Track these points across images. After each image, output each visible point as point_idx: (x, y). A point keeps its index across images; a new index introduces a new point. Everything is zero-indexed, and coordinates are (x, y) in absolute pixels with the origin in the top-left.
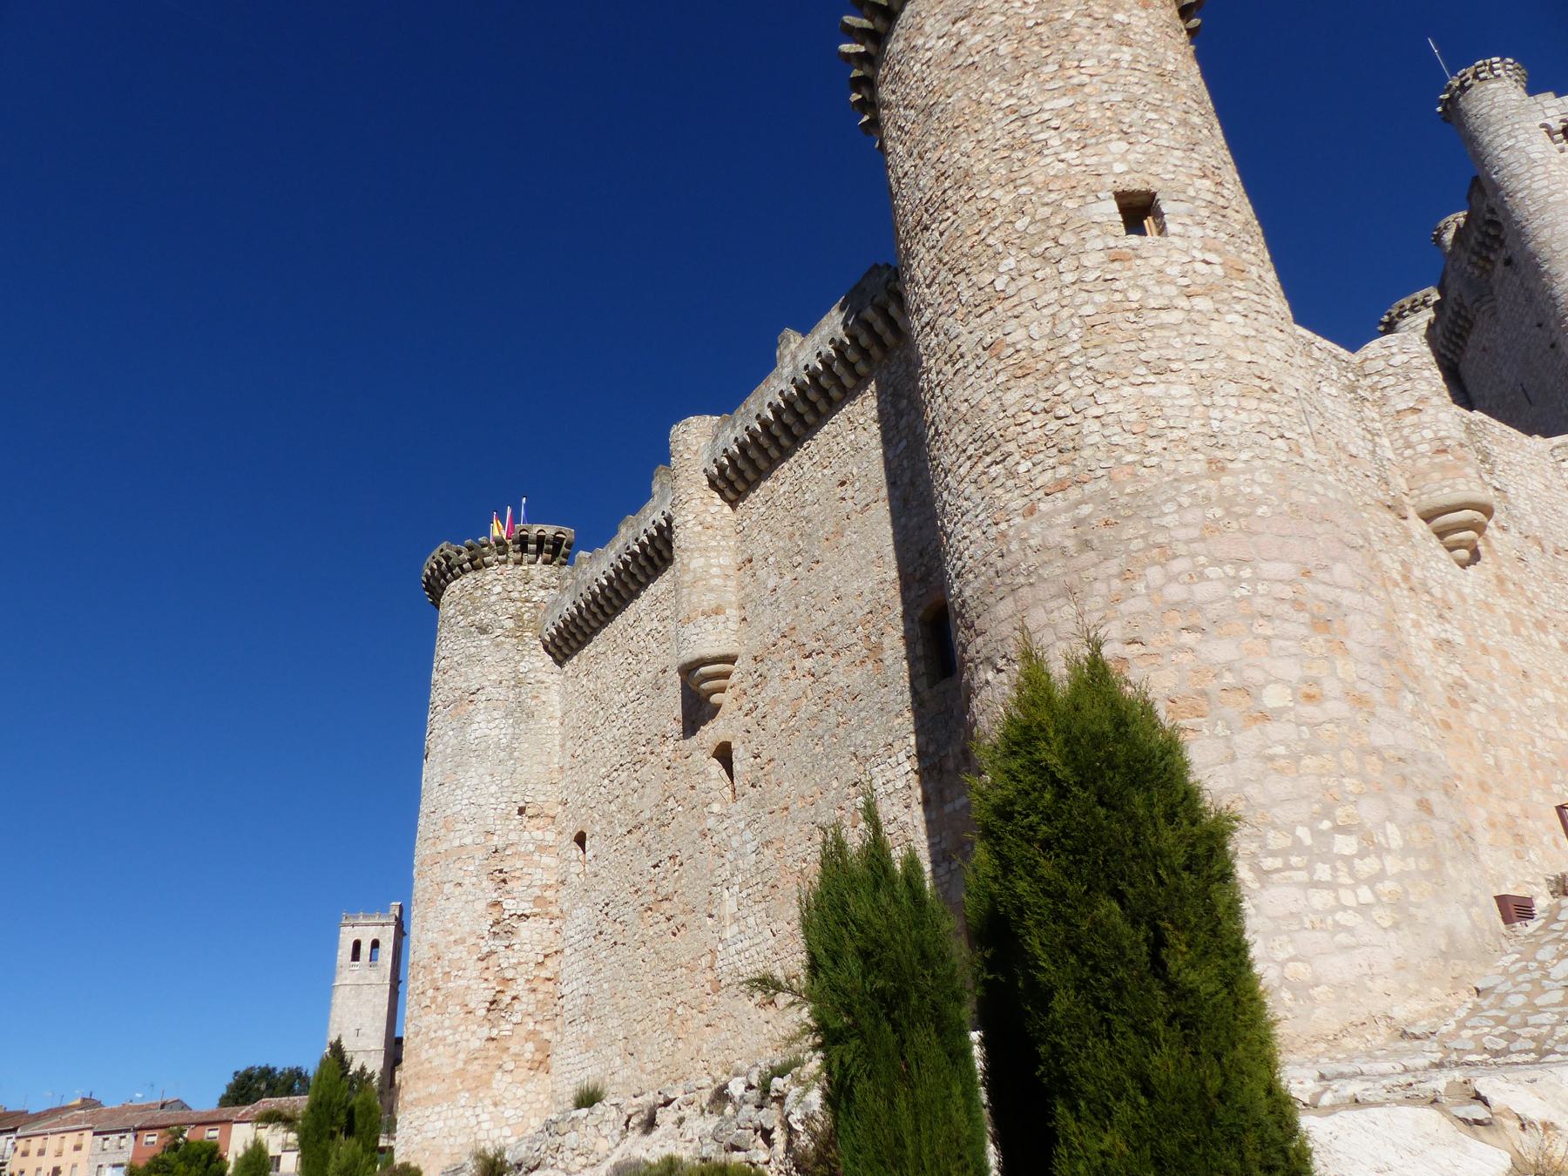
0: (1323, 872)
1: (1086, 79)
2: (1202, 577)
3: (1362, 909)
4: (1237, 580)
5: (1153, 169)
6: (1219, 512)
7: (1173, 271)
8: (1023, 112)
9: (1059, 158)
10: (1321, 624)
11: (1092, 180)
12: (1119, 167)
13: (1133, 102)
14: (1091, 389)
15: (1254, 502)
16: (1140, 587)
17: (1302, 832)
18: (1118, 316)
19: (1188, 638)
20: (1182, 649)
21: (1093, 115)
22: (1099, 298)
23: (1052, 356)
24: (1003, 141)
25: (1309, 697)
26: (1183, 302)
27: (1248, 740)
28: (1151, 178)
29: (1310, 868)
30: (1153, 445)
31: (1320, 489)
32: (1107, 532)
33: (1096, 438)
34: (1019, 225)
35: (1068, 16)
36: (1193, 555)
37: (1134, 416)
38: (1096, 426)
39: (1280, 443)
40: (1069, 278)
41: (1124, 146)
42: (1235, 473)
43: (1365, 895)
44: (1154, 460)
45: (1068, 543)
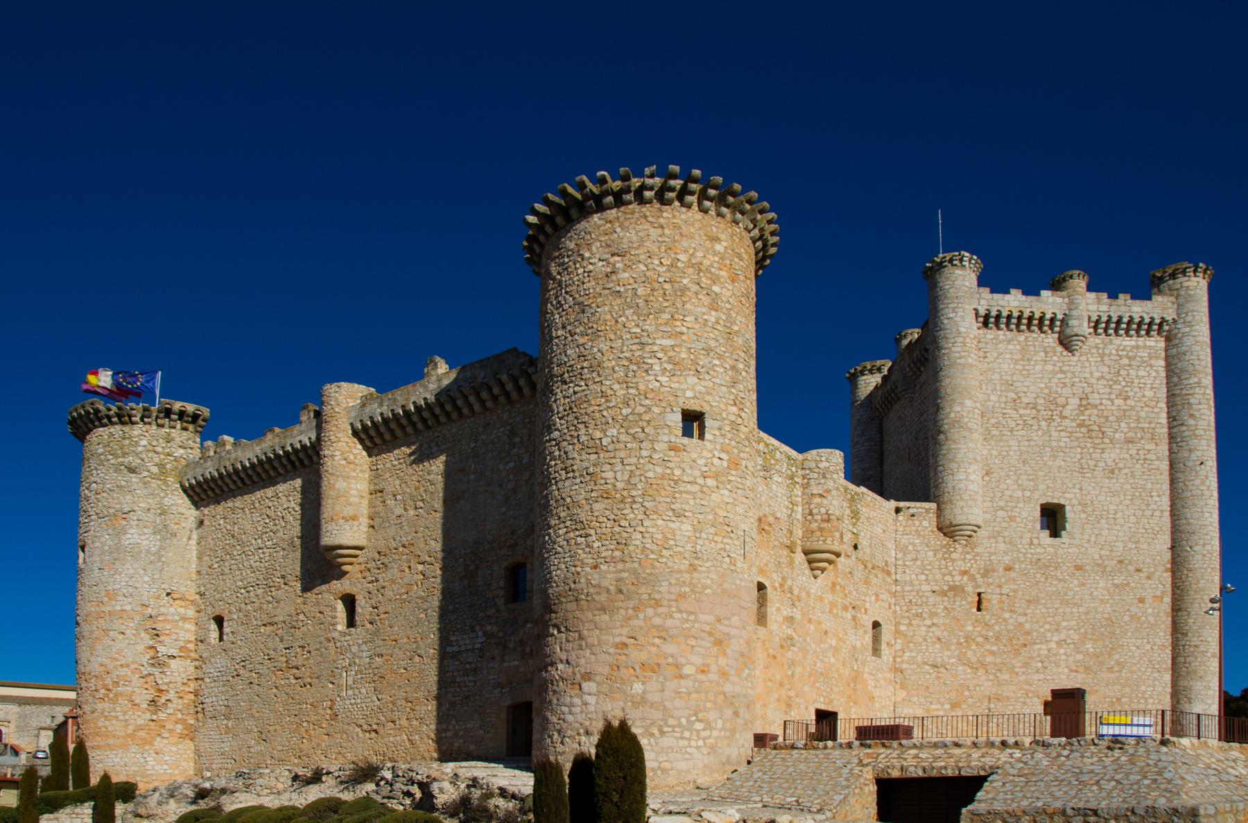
0: (687, 734)
1: (684, 330)
2: (671, 617)
3: (698, 748)
4: (687, 620)
5: (708, 398)
6: (687, 589)
7: (701, 462)
8: (644, 340)
9: (657, 379)
10: (718, 643)
11: (672, 399)
12: (689, 394)
13: (708, 350)
14: (640, 517)
15: (705, 587)
16: (641, 616)
17: (684, 721)
18: (666, 482)
19: (657, 641)
20: (653, 645)
21: (684, 355)
22: (658, 469)
23: (625, 493)
25: (703, 671)
26: (701, 481)
27: (671, 685)
28: (704, 404)
29: (682, 733)
30: (665, 552)
31: (738, 582)
32: (632, 588)
33: (638, 543)
34: (624, 411)
35: (685, 281)
36: (670, 607)
37: (660, 536)
38: (639, 536)
39: (727, 560)
40: (645, 453)
41: (695, 380)
42: (700, 572)
43: (701, 743)
44: (664, 560)
45: (611, 588)
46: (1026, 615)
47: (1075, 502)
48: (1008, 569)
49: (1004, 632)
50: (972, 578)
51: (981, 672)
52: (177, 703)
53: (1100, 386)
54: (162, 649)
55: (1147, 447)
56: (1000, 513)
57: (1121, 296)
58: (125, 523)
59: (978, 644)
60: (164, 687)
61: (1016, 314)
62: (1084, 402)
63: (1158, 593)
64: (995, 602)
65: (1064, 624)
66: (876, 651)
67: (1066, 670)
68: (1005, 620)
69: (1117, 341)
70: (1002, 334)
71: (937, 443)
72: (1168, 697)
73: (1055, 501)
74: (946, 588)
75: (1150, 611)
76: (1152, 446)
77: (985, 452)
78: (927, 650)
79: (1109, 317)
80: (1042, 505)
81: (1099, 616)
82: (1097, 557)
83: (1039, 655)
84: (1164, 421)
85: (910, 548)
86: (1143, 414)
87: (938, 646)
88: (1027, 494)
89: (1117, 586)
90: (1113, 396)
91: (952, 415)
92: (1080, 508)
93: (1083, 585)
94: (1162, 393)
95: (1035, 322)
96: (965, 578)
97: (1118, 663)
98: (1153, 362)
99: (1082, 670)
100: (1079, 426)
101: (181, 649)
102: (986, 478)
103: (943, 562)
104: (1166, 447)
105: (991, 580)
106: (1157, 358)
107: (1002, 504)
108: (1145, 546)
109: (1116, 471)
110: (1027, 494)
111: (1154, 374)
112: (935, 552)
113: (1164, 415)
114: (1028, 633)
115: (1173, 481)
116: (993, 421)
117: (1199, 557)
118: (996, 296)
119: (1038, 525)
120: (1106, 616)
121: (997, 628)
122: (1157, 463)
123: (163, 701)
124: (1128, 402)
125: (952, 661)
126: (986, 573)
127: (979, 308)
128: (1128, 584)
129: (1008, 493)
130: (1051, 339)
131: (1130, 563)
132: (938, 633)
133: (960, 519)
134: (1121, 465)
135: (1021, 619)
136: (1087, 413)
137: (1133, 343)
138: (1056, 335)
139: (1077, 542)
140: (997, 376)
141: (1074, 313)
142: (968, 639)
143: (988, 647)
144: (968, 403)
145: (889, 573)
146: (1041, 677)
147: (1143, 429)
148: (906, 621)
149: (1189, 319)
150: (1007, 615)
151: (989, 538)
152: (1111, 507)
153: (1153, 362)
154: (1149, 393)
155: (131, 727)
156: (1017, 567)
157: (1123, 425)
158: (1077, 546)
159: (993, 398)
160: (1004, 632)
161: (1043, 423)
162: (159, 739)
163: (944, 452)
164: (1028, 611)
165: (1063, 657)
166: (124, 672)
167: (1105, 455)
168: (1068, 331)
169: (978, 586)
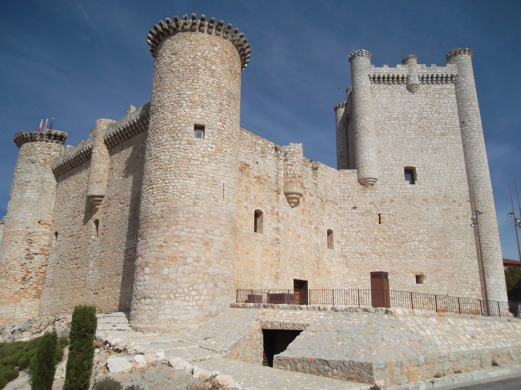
24: (173, 99)
46: (402, 226)
47: (420, 166)
48: (392, 201)
49: (393, 236)
50: (375, 206)
51: (383, 258)
52: (35, 279)
53: (427, 108)
54: (32, 250)
55: (451, 137)
56: (386, 172)
57: (432, 65)
58: (26, 187)
59: (381, 242)
60: (30, 270)
61: (386, 76)
62: (420, 116)
63: (465, 214)
64: (386, 219)
65: (421, 231)
66: (330, 245)
67: (424, 257)
68: (392, 229)
69: (433, 86)
70: (382, 86)
71: (356, 138)
72: (478, 273)
73: (411, 166)
74: (363, 211)
75: (462, 224)
76: (453, 137)
77: (377, 142)
78: (357, 245)
79: (427, 75)
80: (405, 168)
81: (437, 227)
82: (433, 194)
83: (410, 248)
84: (458, 124)
85: (346, 190)
86: (448, 121)
87: (362, 243)
88: (398, 162)
89: (444, 210)
90: (433, 113)
91: (361, 124)
92: (422, 169)
93: (428, 209)
94: (456, 110)
95: (395, 79)
96: (372, 206)
97: (450, 254)
98: (450, 95)
99: (432, 257)
100: (419, 127)
101: (42, 249)
102: (379, 155)
103: (362, 198)
104: (460, 137)
105: (384, 207)
106: (452, 93)
107: (386, 167)
108: (456, 188)
109: (438, 150)
110: (398, 162)
111: (451, 101)
112: (358, 192)
113: (458, 121)
114: (404, 236)
115: (465, 154)
116: (380, 126)
117: (482, 194)
118: (378, 68)
119: (404, 178)
120: (441, 226)
121: (389, 233)
122: (457, 145)
123: (28, 277)
124: (441, 115)
125: (369, 251)
126: (382, 203)
127: (371, 74)
128: (450, 209)
129: (389, 162)
130: (403, 87)
131: (450, 198)
132: (361, 236)
133: (366, 176)
134: (440, 147)
135: (400, 228)
136: (422, 121)
137: (440, 87)
138: (406, 85)
139: (423, 186)
140: (380, 105)
141: (412, 74)
142: (376, 239)
143: (385, 243)
144: (367, 118)
145: (337, 204)
146: (412, 261)
147: (448, 128)
148: (346, 229)
149: (464, 74)
150: (393, 226)
151: (382, 185)
152: (437, 168)
153: (450, 95)
154: (450, 111)
155: (12, 293)
156: (396, 200)
157: (439, 126)
158: (423, 189)
159: (379, 115)
160: (393, 236)
161: (402, 127)
162: (23, 298)
163: (358, 142)
164: (403, 224)
165: (422, 250)
166: (15, 262)
167: (432, 142)
168: (410, 83)
169: (379, 211)
